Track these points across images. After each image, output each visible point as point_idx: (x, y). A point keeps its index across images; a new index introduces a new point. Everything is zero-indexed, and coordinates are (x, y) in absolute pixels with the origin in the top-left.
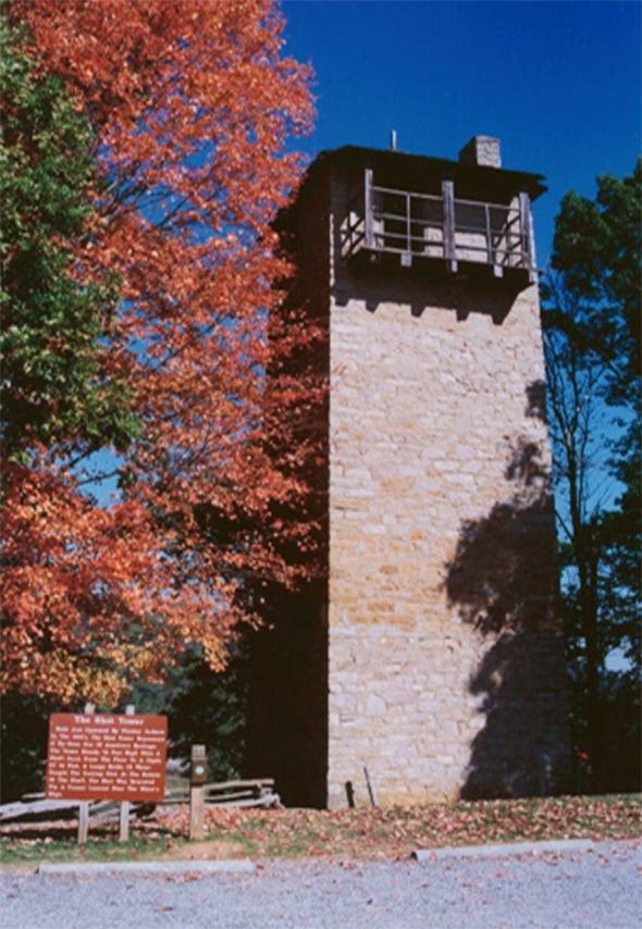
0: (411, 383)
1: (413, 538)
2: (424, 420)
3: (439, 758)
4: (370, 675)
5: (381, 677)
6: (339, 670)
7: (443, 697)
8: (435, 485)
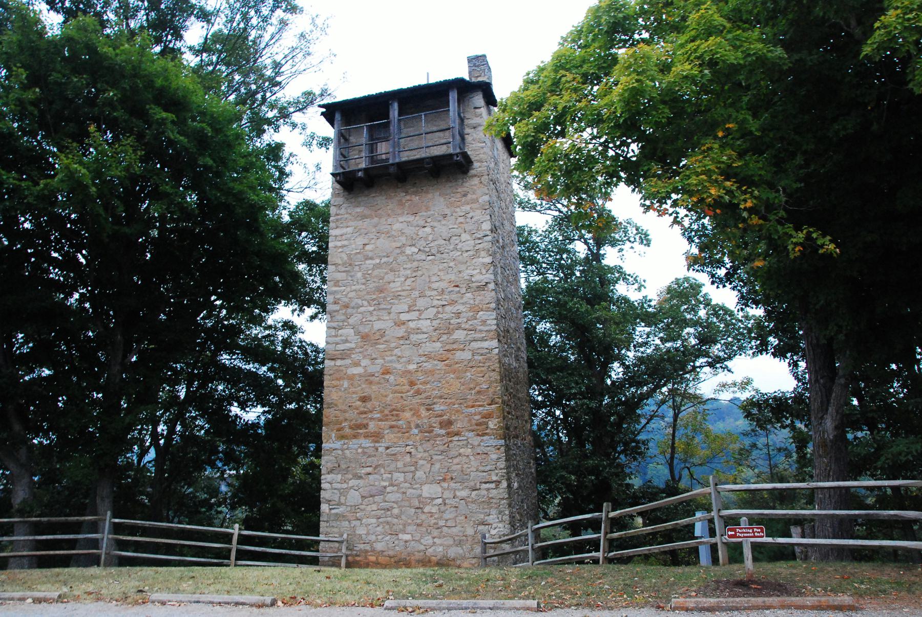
1: (383, 374)
2: (392, 285)
3: (401, 536)
5: (360, 478)
6: (329, 473)
7: (403, 490)
8: (401, 332)
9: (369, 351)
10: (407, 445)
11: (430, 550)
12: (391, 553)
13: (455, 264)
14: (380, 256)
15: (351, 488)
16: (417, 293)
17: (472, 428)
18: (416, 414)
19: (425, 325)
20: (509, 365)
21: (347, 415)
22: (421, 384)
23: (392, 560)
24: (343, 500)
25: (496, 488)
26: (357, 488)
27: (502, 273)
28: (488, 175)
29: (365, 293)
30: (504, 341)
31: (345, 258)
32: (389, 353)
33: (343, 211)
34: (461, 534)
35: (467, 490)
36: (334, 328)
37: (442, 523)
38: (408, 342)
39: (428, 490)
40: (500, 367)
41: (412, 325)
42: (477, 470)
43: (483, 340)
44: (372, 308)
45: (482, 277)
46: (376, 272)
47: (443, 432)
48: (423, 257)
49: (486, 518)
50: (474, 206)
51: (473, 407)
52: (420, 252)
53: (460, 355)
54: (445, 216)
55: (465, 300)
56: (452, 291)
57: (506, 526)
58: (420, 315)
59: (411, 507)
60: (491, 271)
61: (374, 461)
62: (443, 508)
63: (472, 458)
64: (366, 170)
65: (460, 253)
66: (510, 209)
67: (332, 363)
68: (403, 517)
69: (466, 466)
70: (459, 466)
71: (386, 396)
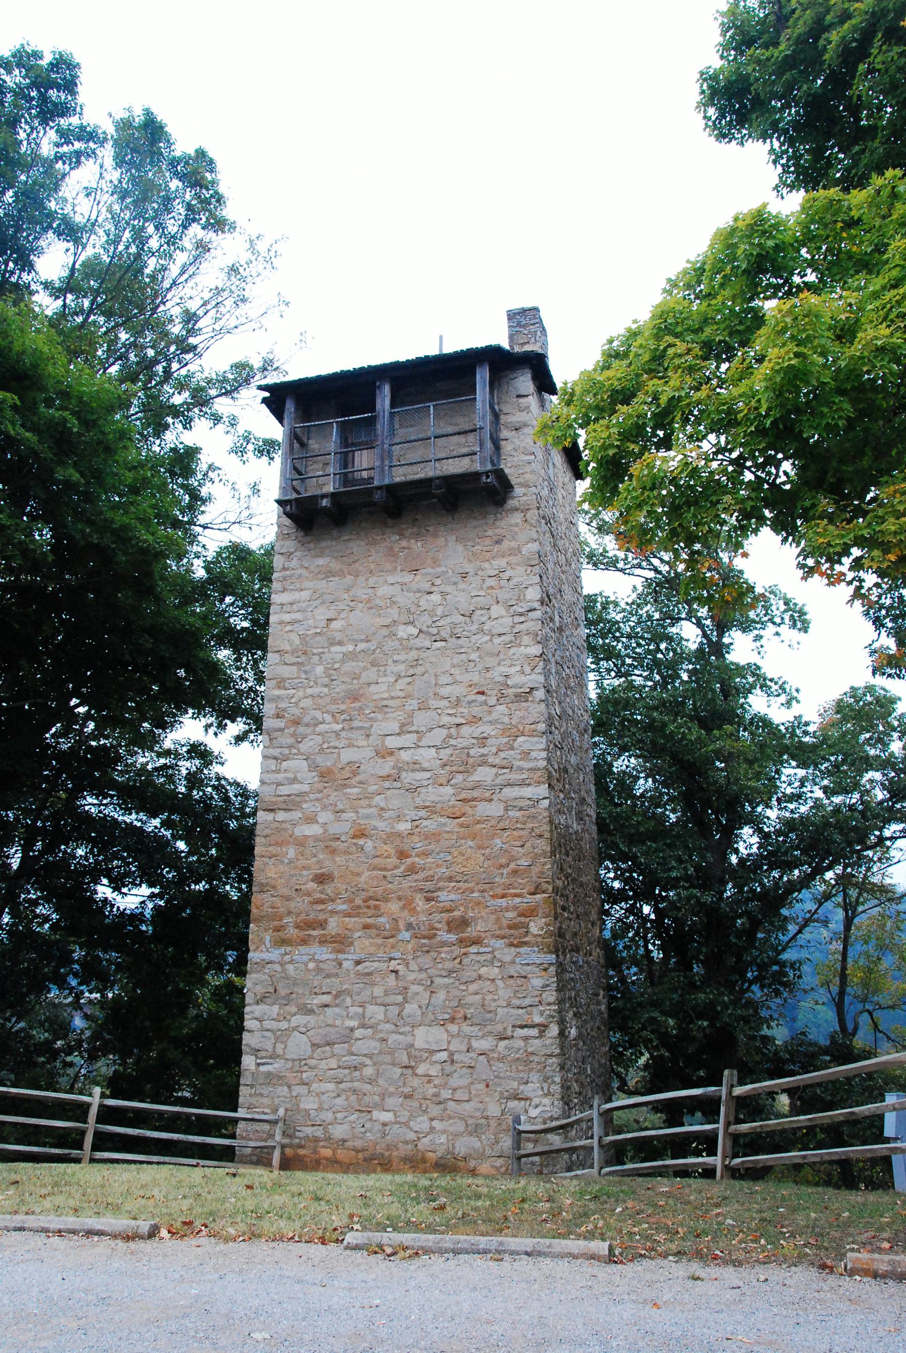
0: (362, 646)
2: (373, 688)
3: (376, 1114)
4: (293, 1009)
5: (311, 1012)
6: (257, 1003)
8: (386, 767)
9: (332, 798)
10: (391, 959)
11: (425, 1141)
12: (358, 1144)
13: (480, 657)
14: (354, 640)
15: (295, 1028)
16: (415, 702)
17: (502, 932)
18: (408, 905)
19: (427, 756)
20: (567, 827)
21: (292, 905)
22: (418, 856)
23: (360, 1155)
24: (279, 1051)
25: (540, 1037)
26: (304, 1030)
27: (557, 673)
28: (538, 508)
29: (328, 700)
30: (559, 786)
31: (297, 641)
32: (366, 802)
33: (294, 563)
34: (478, 1114)
35: (490, 1039)
36: (275, 758)
37: (446, 1094)
38: (398, 784)
39: (424, 1037)
40: (551, 831)
41: (405, 756)
42: (508, 1005)
43: (523, 784)
44: (340, 727)
45: (524, 679)
46: (347, 667)
47: (452, 937)
48: (427, 643)
49: (522, 1087)
50: (514, 559)
51: (503, 897)
52: (421, 635)
53: (484, 809)
54: (464, 575)
55: (494, 716)
56: (473, 701)
57: (556, 1103)
58: (419, 740)
59: (394, 1064)
60: (539, 669)
61: (334, 984)
62: (448, 1068)
63: (500, 983)
64: (333, 496)
65: (488, 638)
66: (573, 566)
67: (270, 816)
68: (381, 1082)
69: (489, 997)
70: (478, 997)
71: (358, 875)
